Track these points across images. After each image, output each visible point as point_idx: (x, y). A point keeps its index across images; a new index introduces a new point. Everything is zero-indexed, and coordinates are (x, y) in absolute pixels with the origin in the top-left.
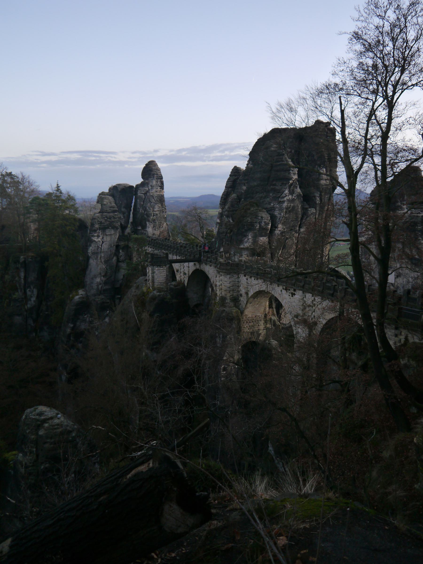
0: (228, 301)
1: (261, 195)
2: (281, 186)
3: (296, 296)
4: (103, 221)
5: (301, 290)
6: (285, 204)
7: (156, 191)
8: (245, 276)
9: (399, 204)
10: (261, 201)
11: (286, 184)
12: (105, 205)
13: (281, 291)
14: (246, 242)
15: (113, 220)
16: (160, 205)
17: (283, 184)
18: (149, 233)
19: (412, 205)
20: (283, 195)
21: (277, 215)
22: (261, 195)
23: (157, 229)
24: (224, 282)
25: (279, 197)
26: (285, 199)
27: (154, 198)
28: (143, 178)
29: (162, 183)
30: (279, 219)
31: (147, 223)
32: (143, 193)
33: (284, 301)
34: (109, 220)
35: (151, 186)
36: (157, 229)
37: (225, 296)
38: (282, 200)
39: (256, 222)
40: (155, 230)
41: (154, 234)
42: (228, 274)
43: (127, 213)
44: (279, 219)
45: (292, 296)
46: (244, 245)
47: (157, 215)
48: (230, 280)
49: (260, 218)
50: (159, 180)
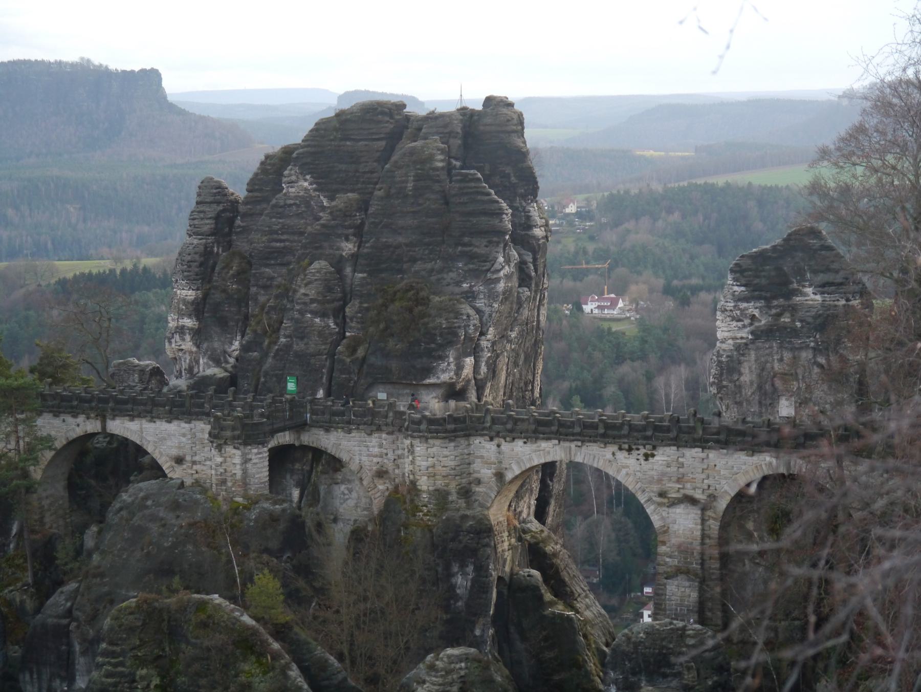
0: (453, 497)
1: (429, 266)
2: (486, 246)
3: (656, 458)
5: (674, 445)
6: (501, 286)
8: (491, 439)
9: (795, 285)
10: (433, 278)
11: (498, 243)
13: (614, 454)
14: (444, 371)
17: (490, 242)
19: (823, 288)
20: (497, 266)
21: (484, 309)
22: (429, 266)
24: (441, 459)
25: (488, 270)
26: (502, 274)
30: (490, 316)
33: (624, 471)
37: (445, 488)
38: (495, 276)
39: (459, 327)
42: (451, 441)
44: (490, 316)
45: (646, 460)
46: (438, 378)
48: (455, 453)
49: (465, 317)
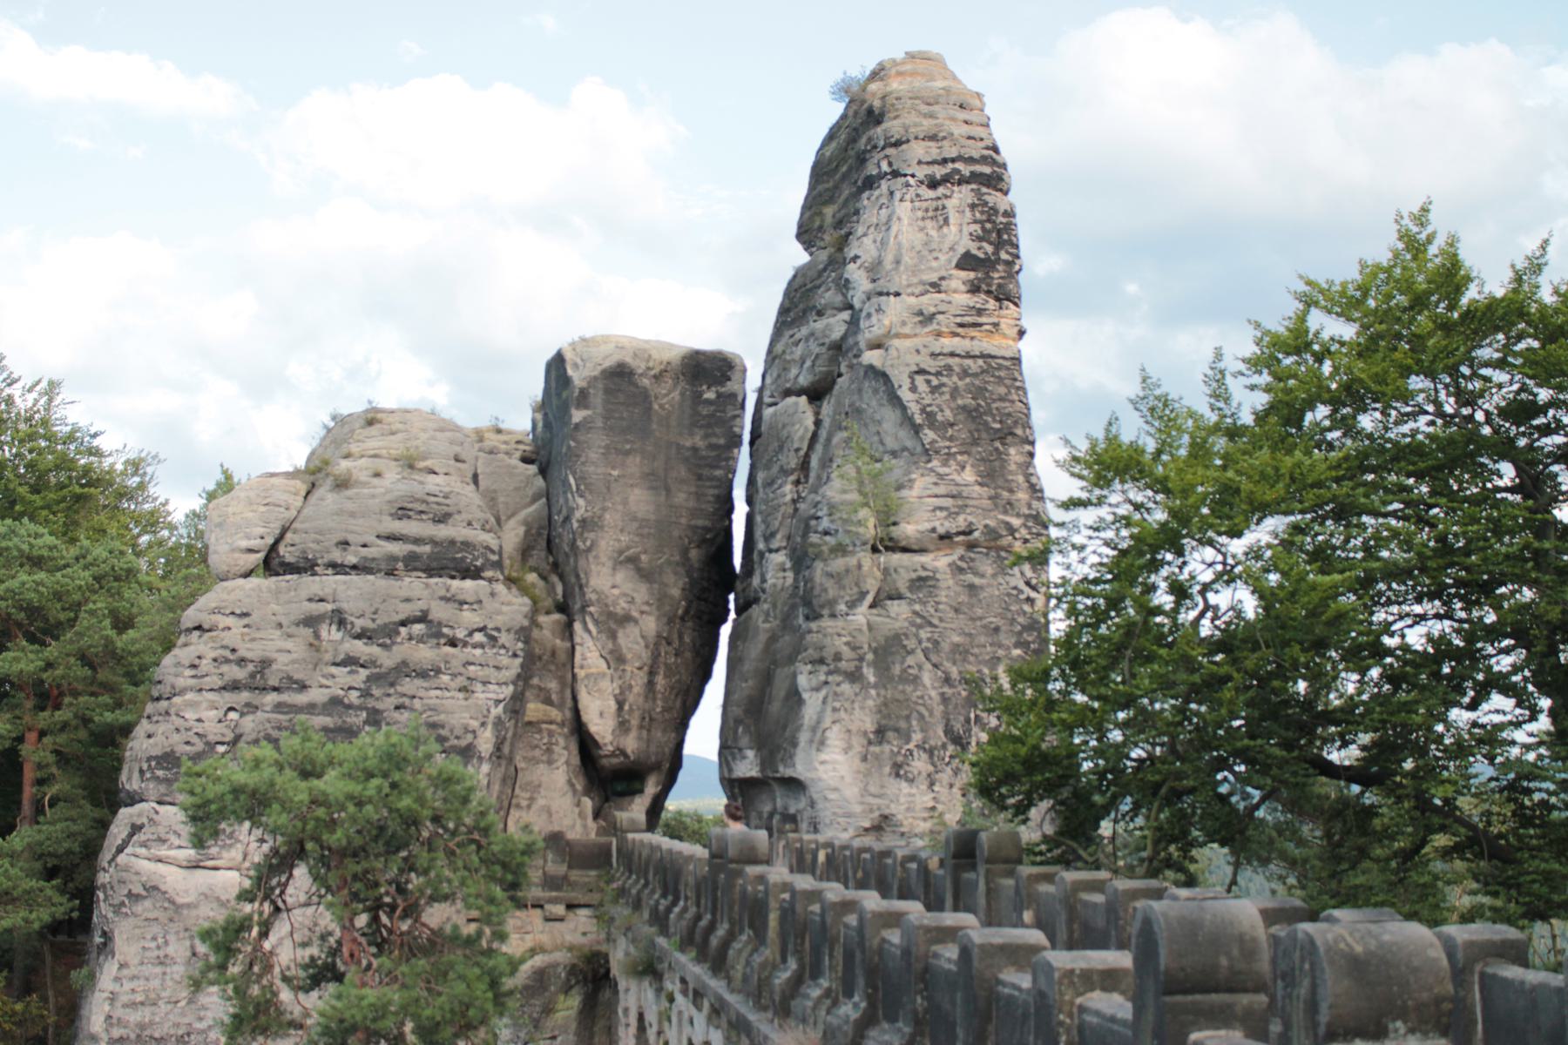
4: (287, 652)
7: (926, 318)
12: (342, 484)
15: (425, 654)
16: (969, 476)
18: (825, 813)
23: (920, 764)
27: (895, 400)
28: (807, 234)
29: (998, 233)
31: (802, 681)
32: (804, 380)
34: (360, 648)
35: (874, 270)
36: (920, 764)
40: (898, 770)
41: (883, 824)
43: (650, 624)
47: (923, 583)
50: (961, 196)
